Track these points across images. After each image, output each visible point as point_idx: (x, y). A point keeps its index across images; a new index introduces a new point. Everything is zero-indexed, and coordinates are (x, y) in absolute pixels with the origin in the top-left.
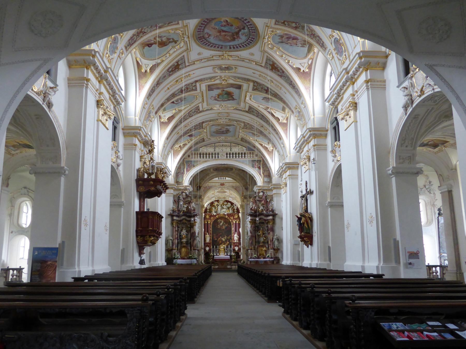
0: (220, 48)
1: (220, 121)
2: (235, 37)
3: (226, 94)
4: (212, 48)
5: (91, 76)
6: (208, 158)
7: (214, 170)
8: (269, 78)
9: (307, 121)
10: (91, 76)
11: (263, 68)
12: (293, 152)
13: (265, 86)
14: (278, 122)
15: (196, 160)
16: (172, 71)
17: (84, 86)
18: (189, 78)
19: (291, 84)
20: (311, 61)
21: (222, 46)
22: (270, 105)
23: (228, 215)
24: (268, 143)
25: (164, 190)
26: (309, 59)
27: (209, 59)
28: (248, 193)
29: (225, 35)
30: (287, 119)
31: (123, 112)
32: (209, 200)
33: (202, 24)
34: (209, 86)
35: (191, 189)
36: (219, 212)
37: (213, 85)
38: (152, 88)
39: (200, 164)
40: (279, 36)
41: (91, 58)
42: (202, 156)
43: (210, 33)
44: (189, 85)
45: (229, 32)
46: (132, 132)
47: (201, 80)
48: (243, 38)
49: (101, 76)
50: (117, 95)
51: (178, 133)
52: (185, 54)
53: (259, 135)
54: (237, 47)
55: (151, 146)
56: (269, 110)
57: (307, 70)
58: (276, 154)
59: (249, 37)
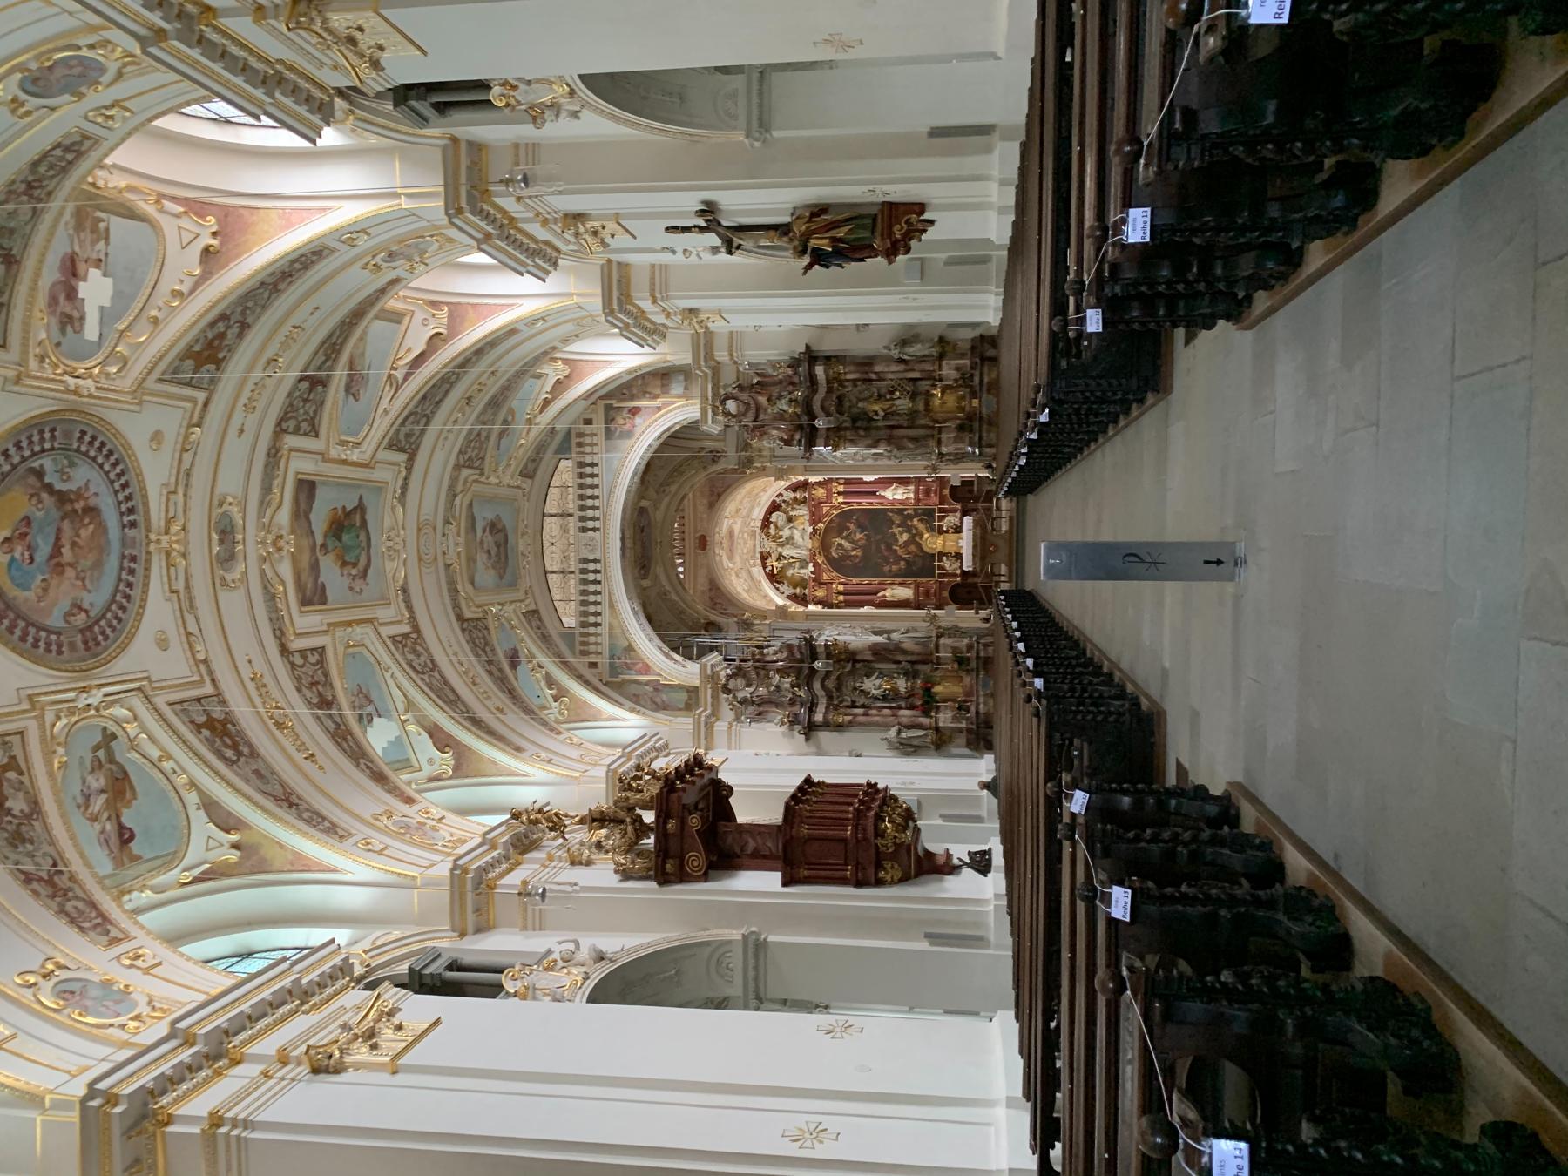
0: (133, 565)
1: (452, 557)
2: (79, 506)
3: (339, 539)
4: (136, 593)
5: (199, 1105)
6: (599, 598)
7: (645, 577)
8: (258, 374)
9: (424, 224)
10: (199, 1105)
11: (215, 397)
12: (556, 282)
13: (295, 388)
14: (445, 341)
15: (605, 640)
16: (235, 747)
17: (238, 1137)
18: (268, 680)
19: (275, 285)
20: (168, 204)
21: (123, 557)
22: (377, 373)
23: (813, 522)
24: (539, 376)
25: (702, 776)
26: (162, 211)
27: (185, 601)
28: (731, 453)
29: (74, 544)
30: (433, 304)
31: (396, 934)
32: (759, 589)
33: (23, 639)
34: (305, 601)
35: (714, 658)
36: (804, 554)
37: (300, 587)
38: (302, 825)
39: (622, 627)
40: (63, 331)
41: (118, 1110)
42: (592, 619)
43: (65, 605)
44: (299, 679)
45: (59, 530)
46: (473, 896)
47: (280, 634)
48: (84, 476)
49: (207, 1057)
50: (304, 981)
51: (501, 710)
52: (160, 701)
53: (502, 414)
54: (128, 498)
55: (537, 822)
56: (399, 374)
57: (212, 220)
58: (580, 348)
59: (78, 450)
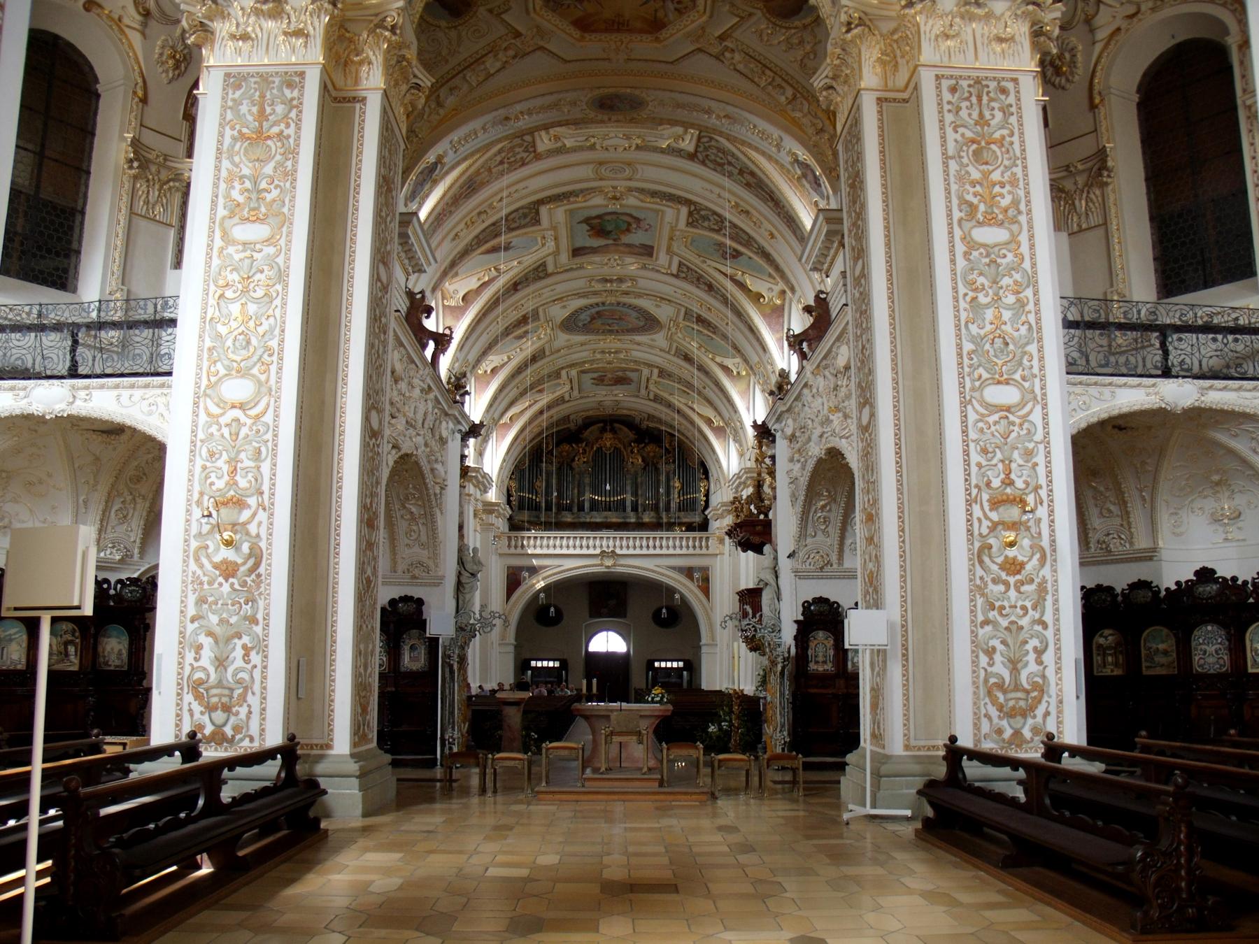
48: (585, 317)
